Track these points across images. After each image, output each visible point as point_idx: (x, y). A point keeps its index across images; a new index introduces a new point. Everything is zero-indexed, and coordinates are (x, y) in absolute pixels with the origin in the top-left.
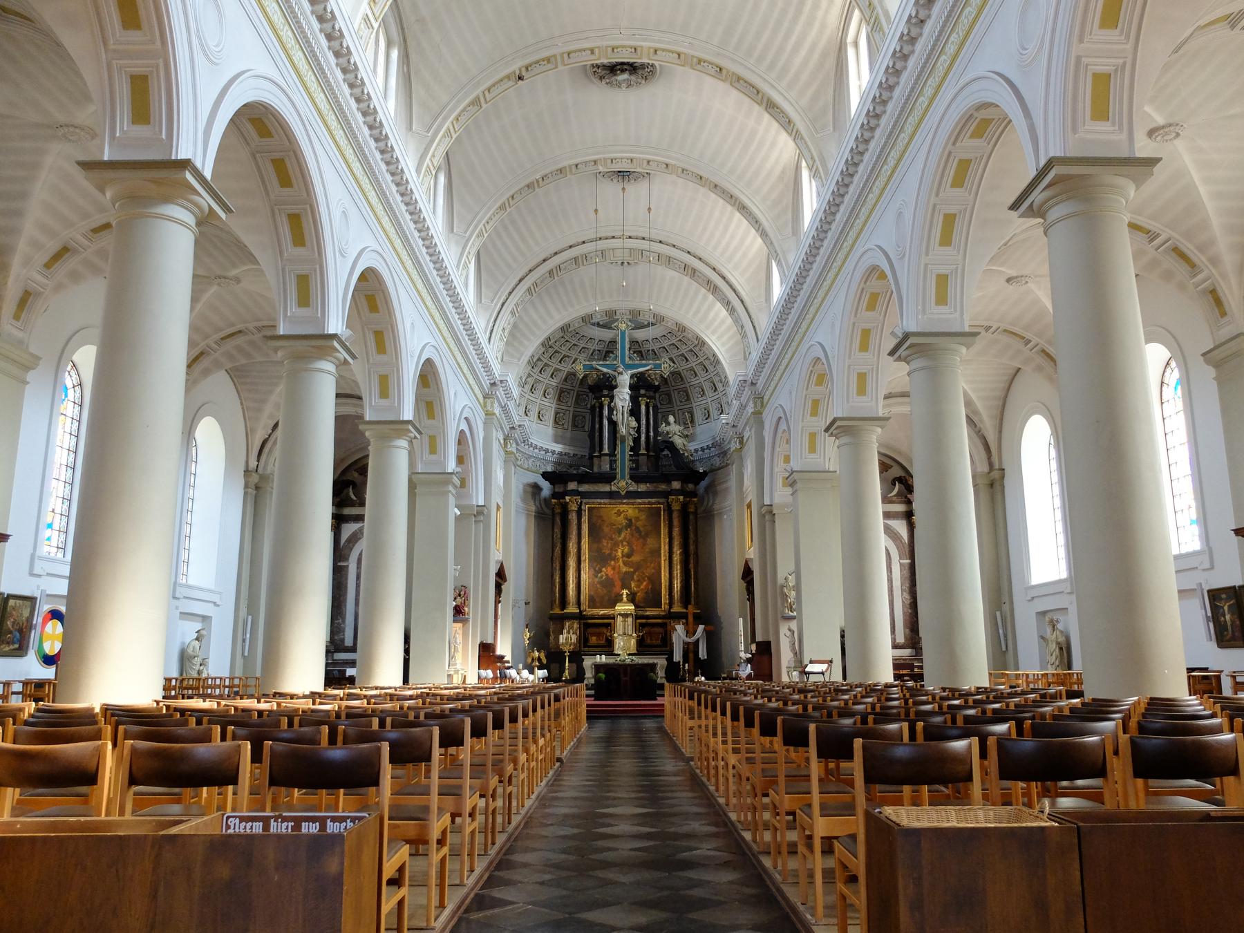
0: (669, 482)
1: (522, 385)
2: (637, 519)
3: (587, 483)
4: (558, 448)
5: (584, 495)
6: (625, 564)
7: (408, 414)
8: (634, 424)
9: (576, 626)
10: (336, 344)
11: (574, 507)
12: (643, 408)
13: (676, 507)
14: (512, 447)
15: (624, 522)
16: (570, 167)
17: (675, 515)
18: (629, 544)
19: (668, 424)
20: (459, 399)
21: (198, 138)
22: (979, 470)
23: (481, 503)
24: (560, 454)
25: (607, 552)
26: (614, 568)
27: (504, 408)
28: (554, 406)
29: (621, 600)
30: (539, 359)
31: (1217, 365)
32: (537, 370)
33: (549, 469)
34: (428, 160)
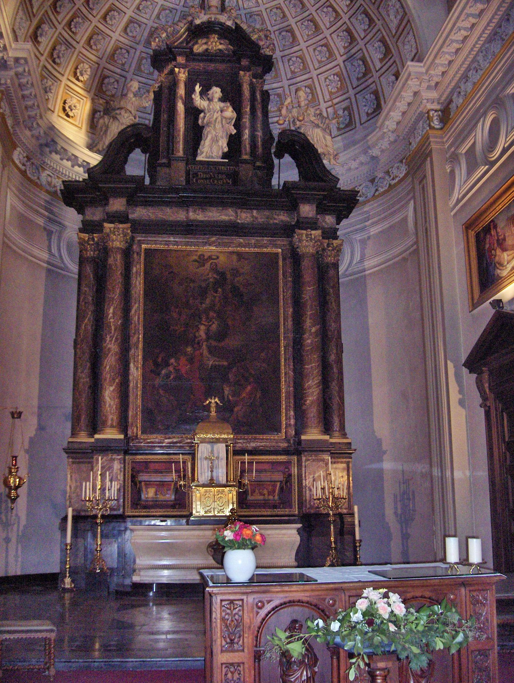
0: (293, 207)
2: (236, 272)
15: (212, 277)
18: (220, 315)
25: (179, 329)
26: (191, 360)
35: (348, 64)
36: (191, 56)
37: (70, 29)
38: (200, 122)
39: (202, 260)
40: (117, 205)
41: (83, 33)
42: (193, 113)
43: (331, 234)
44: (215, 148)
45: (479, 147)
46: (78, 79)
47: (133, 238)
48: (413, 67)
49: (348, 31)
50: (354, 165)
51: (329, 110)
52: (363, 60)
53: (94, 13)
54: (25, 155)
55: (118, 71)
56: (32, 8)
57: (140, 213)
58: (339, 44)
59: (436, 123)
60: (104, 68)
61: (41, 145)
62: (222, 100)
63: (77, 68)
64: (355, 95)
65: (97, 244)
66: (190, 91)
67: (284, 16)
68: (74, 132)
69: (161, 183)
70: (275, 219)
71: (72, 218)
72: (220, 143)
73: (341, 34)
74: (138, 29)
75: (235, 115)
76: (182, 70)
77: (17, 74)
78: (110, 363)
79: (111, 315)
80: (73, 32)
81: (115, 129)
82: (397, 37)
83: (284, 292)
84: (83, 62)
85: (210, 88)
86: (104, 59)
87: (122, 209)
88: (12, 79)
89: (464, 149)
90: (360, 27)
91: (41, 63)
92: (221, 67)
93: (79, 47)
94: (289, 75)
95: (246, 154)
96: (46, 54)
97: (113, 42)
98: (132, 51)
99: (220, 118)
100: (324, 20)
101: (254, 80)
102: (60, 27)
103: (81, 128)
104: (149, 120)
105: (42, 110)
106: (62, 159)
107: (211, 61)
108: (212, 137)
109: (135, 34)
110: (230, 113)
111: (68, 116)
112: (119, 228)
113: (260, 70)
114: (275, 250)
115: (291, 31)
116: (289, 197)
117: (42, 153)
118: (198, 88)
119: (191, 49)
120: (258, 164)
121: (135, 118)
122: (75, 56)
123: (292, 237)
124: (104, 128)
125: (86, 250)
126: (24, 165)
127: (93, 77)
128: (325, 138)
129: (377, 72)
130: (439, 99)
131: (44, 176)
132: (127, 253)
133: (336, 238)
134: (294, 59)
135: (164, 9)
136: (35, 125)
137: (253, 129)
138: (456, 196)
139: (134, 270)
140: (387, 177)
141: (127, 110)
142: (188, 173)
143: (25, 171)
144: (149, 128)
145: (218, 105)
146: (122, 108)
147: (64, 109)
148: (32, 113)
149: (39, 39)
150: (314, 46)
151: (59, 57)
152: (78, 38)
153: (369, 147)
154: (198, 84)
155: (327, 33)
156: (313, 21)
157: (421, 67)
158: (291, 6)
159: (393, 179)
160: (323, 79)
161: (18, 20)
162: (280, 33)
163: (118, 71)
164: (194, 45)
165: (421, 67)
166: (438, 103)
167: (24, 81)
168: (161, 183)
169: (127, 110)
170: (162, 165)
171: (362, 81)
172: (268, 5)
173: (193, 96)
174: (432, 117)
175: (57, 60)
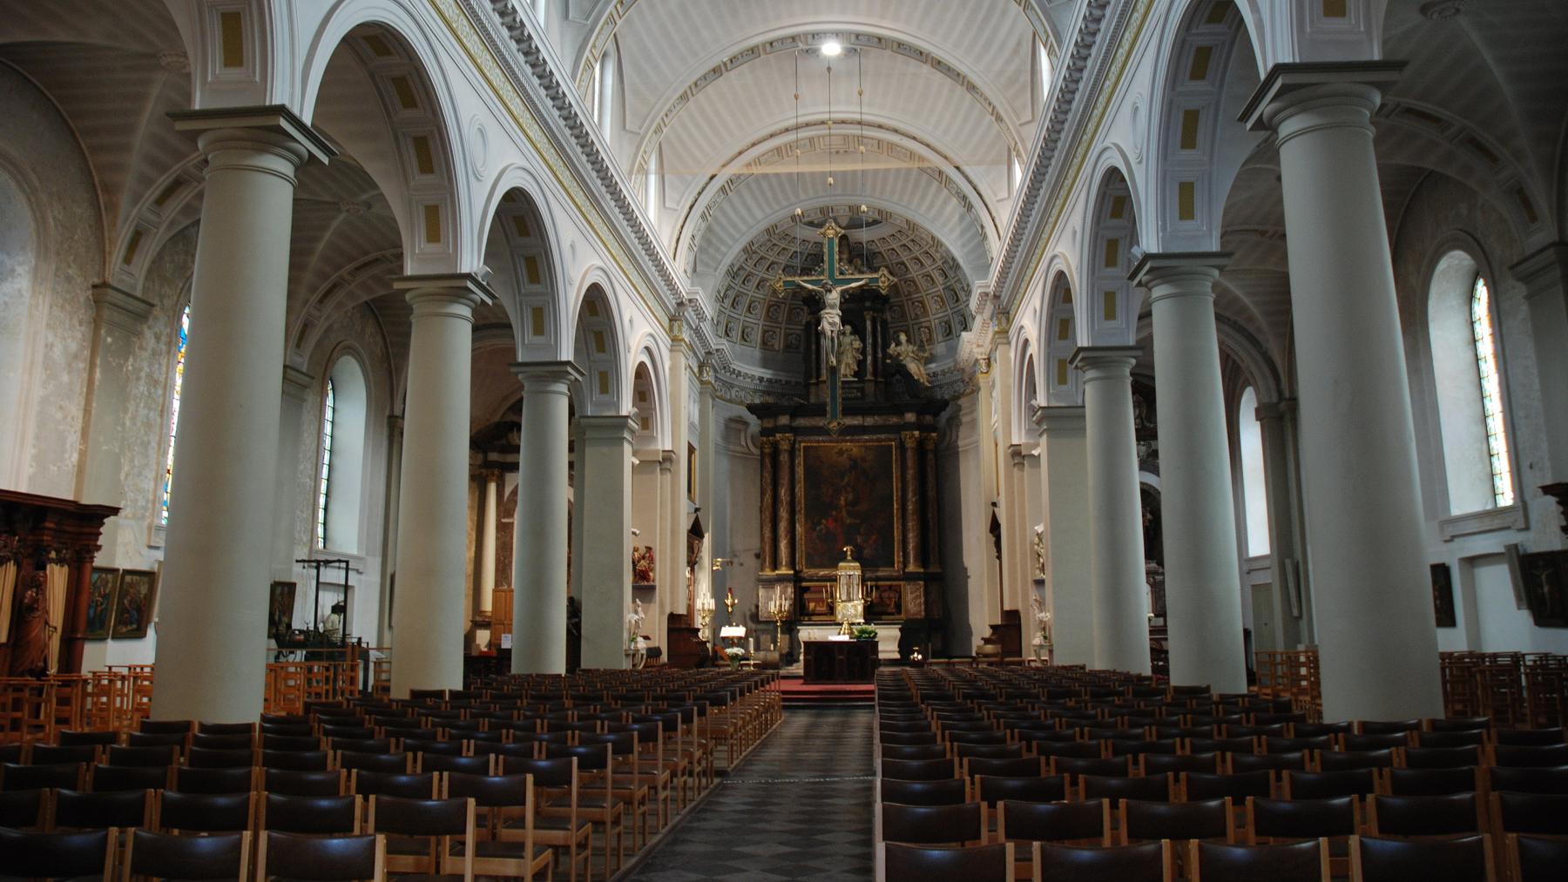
0: (902, 414)
1: (720, 299)
2: (864, 460)
3: (803, 416)
4: (767, 374)
6: (849, 513)
7: (567, 353)
8: (857, 344)
9: (790, 590)
10: (470, 285)
11: (785, 446)
12: (869, 324)
13: (910, 444)
14: (709, 376)
16: (764, 45)
17: (909, 454)
19: (898, 344)
20: (638, 330)
21: (295, 82)
22: (1266, 400)
23: (668, 447)
24: (769, 380)
27: (697, 332)
28: (761, 323)
29: (844, 559)
30: (741, 268)
31: (1526, 279)
32: (739, 280)
33: (757, 401)
34: (587, 53)
39: (841, 452)
40: (784, 420)
57: (802, 422)
78: (783, 526)
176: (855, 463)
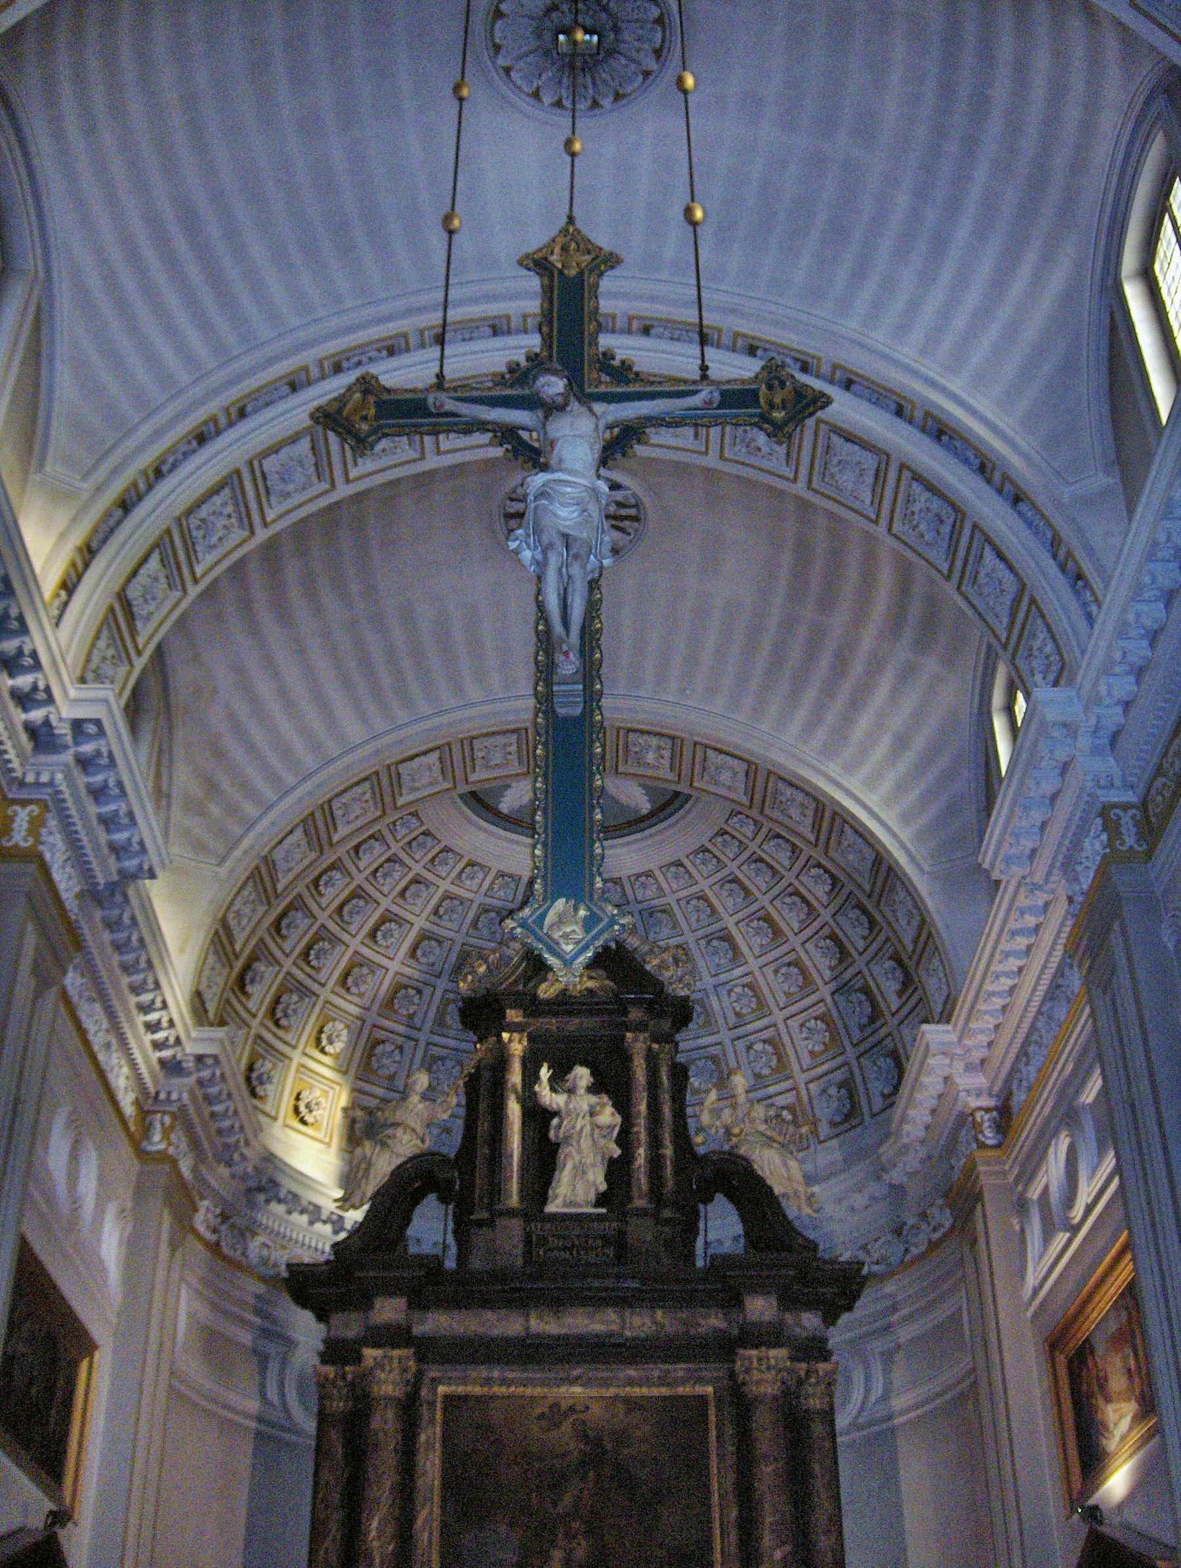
0: (733, 1301)
2: (621, 1437)
5: (428, 1350)
35: (841, 1000)
36: (534, 1007)
37: (308, 963)
38: (552, 1134)
39: (555, 1415)
41: (334, 964)
42: (538, 1118)
43: (814, 1350)
44: (580, 1188)
45: (1055, 1196)
46: (323, 1051)
47: (419, 1375)
48: (933, 1033)
49: (833, 937)
50: (860, 1200)
51: (811, 1086)
52: (866, 990)
53: (353, 929)
54: (218, 1211)
55: (401, 1029)
56: (232, 943)
57: (438, 1323)
58: (820, 962)
59: (989, 1136)
60: (375, 1026)
61: (249, 1191)
62: (593, 1089)
63: (321, 1031)
64: (858, 1058)
65: (352, 1385)
66: (531, 1077)
67: (714, 911)
68: (313, 1155)
69: (476, 1263)
70: (698, 1325)
71: (306, 1330)
72: (590, 1176)
73: (822, 943)
74: (437, 951)
75: (618, 1119)
76: (516, 1036)
77: (201, 1083)
79: (373, 1534)
80: (313, 967)
81: (384, 1165)
82: (915, 958)
83: (720, 1479)
84: (334, 1020)
85: (570, 1069)
86: (375, 1008)
87: (400, 1317)
88: (191, 1092)
89: (1034, 1193)
90: (855, 935)
91: (253, 1032)
92: (589, 1022)
93: (325, 994)
94: (732, 1020)
95: (640, 1197)
96: (260, 1015)
97: (391, 974)
98: (427, 991)
99: (588, 1129)
100: (789, 918)
101: (656, 1046)
102: (288, 964)
103: (328, 1144)
104: (451, 1146)
105: (249, 1131)
106: (289, 1212)
107: (570, 1013)
108: (574, 1167)
109: (432, 959)
110: (608, 1116)
111: (303, 1122)
112: (392, 1358)
113: (666, 1025)
114: (699, 1390)
115: (727, 938)
116: (725, 1284)
117: (252, 1205)
118: (545, 1073)
119: (535, 996)
120: (667, 1213)
121: (423, 1141)
122: (317, 1010)
123: (733, 1361)
124: (363, 1166)
125: (331, 1398)
126: (215, 1231)
127: (353, 1044)
128: (785, 1164)
129: (893, 1015)
130: (990, 1089)
131: (255, 1246)
132: (409, 1408)
133: (825, 1355)
134: (738, 990)
135: (487, 911)
136: (236, 1156)
137: (655, 1143)
138: (1031, 1280)
139: (423, 1438)
140: (924, 1227)
141: (406, 1127)
142: (528, 1242)
143: (218, 1244)
144: (449, 1160)
145: (584, 1101)
146: (398, 1124)
147: (296, 1111)
148: (232, 1140)
149: (249, 988)
150: (773, 966)
151: (286, 1015)
152: (322, 977)
153: (884, 1169)
154: (545, 1065)
155: (795, 941)
156: (768, 919)
157: (947, 1032)
158: (725, 893)
159: (935, 1230)
160: (796, 1025)
161: (206, 973)
162: (708, 943)
163: (401, 1029)
164: (540, 983)
165: (947, 1032)
166: (990, 1095)
167: (213, 1090)
168: (476, 1263)
169: (406, 1127)
170: (480, 1224)
171: (869, 1030)
172: (680, 894)
173: (537, 1088)
174: (981, 1124)
175: (283, 1022)
176: (597, 1450)
